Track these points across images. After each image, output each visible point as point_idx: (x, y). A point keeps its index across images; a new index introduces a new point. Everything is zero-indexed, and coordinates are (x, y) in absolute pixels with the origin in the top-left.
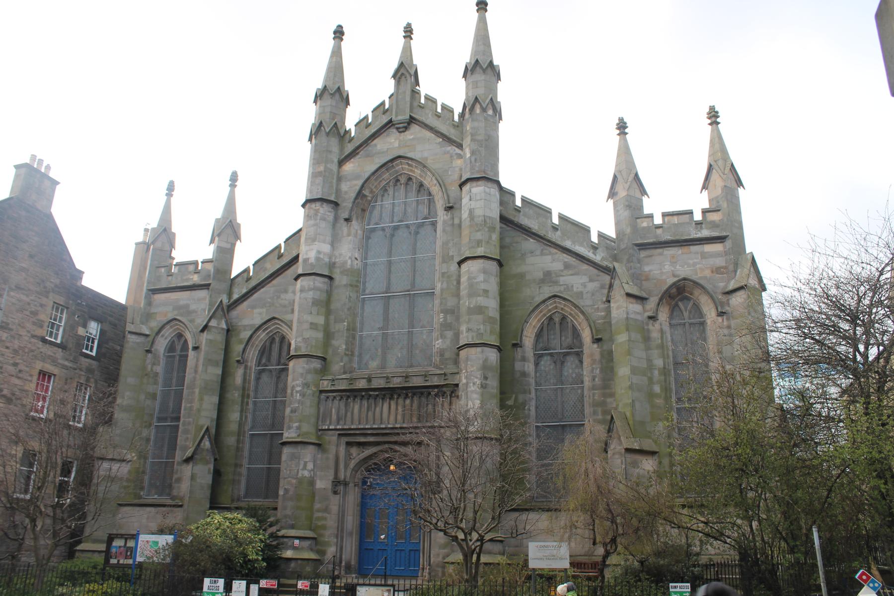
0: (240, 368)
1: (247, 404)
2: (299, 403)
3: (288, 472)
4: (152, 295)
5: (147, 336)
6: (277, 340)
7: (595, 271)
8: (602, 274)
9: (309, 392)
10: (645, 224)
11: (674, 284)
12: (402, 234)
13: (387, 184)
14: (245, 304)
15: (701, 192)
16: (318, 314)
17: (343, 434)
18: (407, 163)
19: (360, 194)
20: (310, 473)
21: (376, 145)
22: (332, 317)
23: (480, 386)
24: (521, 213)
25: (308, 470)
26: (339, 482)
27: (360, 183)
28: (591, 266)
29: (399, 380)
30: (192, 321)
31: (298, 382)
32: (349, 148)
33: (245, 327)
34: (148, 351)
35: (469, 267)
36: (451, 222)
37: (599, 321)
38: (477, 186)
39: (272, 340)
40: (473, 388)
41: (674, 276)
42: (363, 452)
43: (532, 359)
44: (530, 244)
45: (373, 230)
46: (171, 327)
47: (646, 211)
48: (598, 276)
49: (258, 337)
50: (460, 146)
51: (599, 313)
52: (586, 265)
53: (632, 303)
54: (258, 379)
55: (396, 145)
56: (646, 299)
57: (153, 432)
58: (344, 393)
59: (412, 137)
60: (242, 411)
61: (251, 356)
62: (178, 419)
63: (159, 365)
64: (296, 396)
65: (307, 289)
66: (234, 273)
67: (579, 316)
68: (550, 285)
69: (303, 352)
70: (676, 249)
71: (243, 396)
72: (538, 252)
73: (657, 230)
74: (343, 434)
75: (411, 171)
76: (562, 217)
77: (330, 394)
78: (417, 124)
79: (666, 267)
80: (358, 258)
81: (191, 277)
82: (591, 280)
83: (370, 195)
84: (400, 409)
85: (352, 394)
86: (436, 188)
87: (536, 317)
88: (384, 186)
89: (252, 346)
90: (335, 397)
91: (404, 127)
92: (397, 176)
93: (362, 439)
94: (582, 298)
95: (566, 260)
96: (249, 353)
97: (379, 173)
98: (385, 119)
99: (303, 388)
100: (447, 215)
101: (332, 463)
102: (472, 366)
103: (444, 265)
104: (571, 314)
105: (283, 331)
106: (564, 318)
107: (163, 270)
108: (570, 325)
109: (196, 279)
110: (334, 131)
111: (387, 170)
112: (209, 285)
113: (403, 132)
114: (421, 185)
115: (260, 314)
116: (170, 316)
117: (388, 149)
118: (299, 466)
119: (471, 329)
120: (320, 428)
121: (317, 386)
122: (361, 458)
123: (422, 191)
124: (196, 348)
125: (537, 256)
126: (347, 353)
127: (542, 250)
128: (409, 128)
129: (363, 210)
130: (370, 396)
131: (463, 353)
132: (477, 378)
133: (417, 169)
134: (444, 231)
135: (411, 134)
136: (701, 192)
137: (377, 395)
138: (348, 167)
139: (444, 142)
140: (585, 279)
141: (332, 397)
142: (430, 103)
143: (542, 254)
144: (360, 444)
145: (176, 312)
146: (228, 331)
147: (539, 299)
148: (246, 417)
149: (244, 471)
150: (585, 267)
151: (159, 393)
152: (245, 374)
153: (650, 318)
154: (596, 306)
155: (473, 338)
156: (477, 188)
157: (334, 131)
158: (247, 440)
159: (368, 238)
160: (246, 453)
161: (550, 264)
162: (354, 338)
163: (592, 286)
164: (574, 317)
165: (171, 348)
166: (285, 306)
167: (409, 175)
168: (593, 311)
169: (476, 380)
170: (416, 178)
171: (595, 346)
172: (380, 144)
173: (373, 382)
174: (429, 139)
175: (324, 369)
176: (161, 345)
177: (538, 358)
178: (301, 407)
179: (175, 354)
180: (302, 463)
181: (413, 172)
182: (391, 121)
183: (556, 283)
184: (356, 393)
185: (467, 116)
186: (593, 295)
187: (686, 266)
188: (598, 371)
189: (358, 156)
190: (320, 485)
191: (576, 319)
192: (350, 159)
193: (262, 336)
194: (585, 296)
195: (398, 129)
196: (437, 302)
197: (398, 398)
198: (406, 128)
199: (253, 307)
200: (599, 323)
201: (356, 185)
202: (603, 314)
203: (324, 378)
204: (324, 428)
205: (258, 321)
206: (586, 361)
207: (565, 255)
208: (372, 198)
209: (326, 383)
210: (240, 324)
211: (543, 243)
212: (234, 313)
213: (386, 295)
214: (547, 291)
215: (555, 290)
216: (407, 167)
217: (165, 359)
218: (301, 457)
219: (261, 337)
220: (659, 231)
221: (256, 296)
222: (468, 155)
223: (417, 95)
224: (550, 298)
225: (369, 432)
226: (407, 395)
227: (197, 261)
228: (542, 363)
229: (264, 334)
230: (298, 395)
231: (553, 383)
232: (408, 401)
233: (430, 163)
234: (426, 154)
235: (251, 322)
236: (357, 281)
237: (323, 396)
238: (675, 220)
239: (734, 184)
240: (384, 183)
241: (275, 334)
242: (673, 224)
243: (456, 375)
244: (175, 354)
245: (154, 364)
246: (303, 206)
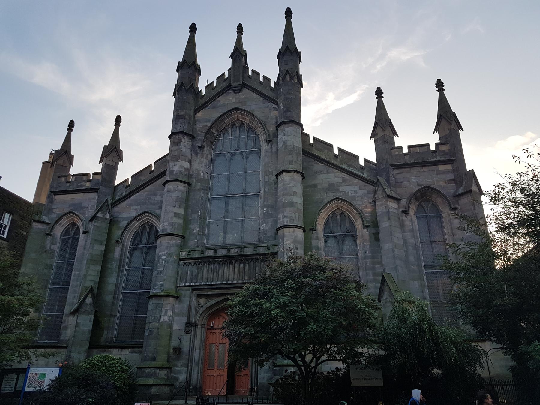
0: (118, 247)
1: (123, 271)
2: (164, 268)
3: (153, 318)
4: (54, 196)
5: (48, 224)
6: (147, 227)
7: (364, 183)
8: (367, 185)
9: (172, 259)
10: (397, 153)
11: (419, 190)
12: (238, 158)
13: (227, 126)
17: (195, 288)
19: (209, 131)
20: (170, 318)
21: (219, 101)
22: (190, 210)
24: (314, 148)
25: (168, 316)
26: (191, 324)
27: (209, 124)
28: (360, 180)
29: (236, 250)
30: (84, 214)
31: (163, 253)
32: (201, 102)
33: (124, 219)
34: (48, 235)
35: (286, 177)
36: (270, 151)
37: (367, 215)
39: (143, 227)
41: (418, 185)
42: (209, 301)
43: (323, 239)
44: (320, 166)
45: (218, 155)
46: (67, 218)
47: (397, 145)
48: (365, 186)
49: (134, 225)
50: (276, 103)
51: (367, 210)
53: (391, 202)
54: (132, 254)
56: (401, 200)
57: (48, 292)
58: (197, 261)
59: (244, 96)
60: (118, 276)
61: (127, 238)
62: (69, 283)
63: (56, 245)
64: (162, 262)
65: (172, 190)
66: (117, 183)
67: (353, 212)
69: (169, 231)
70: (419, 168)
71: (120, 266)
72: (325, 172)
73: (405, 156)
74: (195, 288)
75: (243, 118)
77: (187, 261)
79: (413, 180)
80: (208, 172)
81: (85, 184)
83: (216, 133)
84: (236, 270)
85: (204, 260)
86: (260, 129)
87: (325, 212)
88: (225, 128)
89: (129, 231)
90: (190, 263)
91: (238, 90)
93: (209, 292)
94: (355, 200)
95: (344, 176)
96: (126, 236)
98: (225, 85)
99: (168, 257)
100: (268, 146)
101: (185, 310)
102: (287, 240)
103: (267, 177)
104: (347, 210)
105: (153, 221)
106: (343, 213)
107: (63, 179)
108: (347, 217)
109: (88, 185)
112: (99, 189)
113: (238, 93)
114: (250, 128)
115: (136, 209)
116: (67, 210)
117: (228, 103)
118: (162, 314)
119: (286, 217)
120: (179, 285)
123: (250, 132)
124: (85, 232)
126: (200, 233)
127: (328, 170)
128: (242, 91)
129: (212, 143)
130: (216, 261)
131: (280, 232)
133: (248, 117)
134: (266, 156)
137: (221, 261)
138: (199, 114)
139: (265, 100)
140: (356, 188)
141: (188, 263)
142: (255, 75)
143: (328, 173)
144: (207, 296)
145: (71, 208)
146: (111, 220)
147: (326, 201)
148: (121, 281)
149: (117, 320)
150: (357, 180)
153: (403, 212)
154: (365, 205)
155: (287, 222)
156: (288, 128)
158: (121, 297)
159: (215, 160)
160: (119, 306)
161: (333, 179)
162: (205, 223)
163: (361, 192)
164: (350, 212)
165: (66, 233)
166: (154, 204)
168: (363, 208)
170: (247, 123)
171: (366, 230)
172: (222, 100)
173: (218, 252)
174: (255, 98)
176: (59, 231)
177: (327, 238)
178: (165, 270)
179: (69, 237)
180: (164, 311)
181: (245, 119)
182: (230, 85)
183: (338, 191)
185: (281, 83)
186: (362, 198)
188: (368, 247)
189: (208, 107)
190: (175, 327)
194: (357, 199)
195: (234, 91)
196: (262, 200)
197: (235, 263)
198: (240, 91)
199: (131, 205)
200: (367, 216)
201: (206, 126)
202: (369, 210)
203: (182, 250)
204: (181, 285)
205: (134, 214)
207: (343, 173)
208: (217, 135)
209: (184, 253)
210: (120, 216)
211: (329, 166)
212: (116, 209)
213: (227, 196)
214: (331, 196)
215: (338, 195)
216: (241, 116)
217: (61, 240)
218: (164, 307)
220: (407, 158)
222: (282, 107)
223: (247, 70)
227: (90, 173)
230: (164, 262)
231: (337, 255)
232: (242, 265)
233: (256, 113)
234: (253, 107)
235: (129, 215)
236: (207, 187)
237: (182, 262)
238: (418, 150)
240: (225, 125)
242: (417, 153)
243: (276, 246)
244: (69, 237)
245: (52, 244)
246: (170, 137)
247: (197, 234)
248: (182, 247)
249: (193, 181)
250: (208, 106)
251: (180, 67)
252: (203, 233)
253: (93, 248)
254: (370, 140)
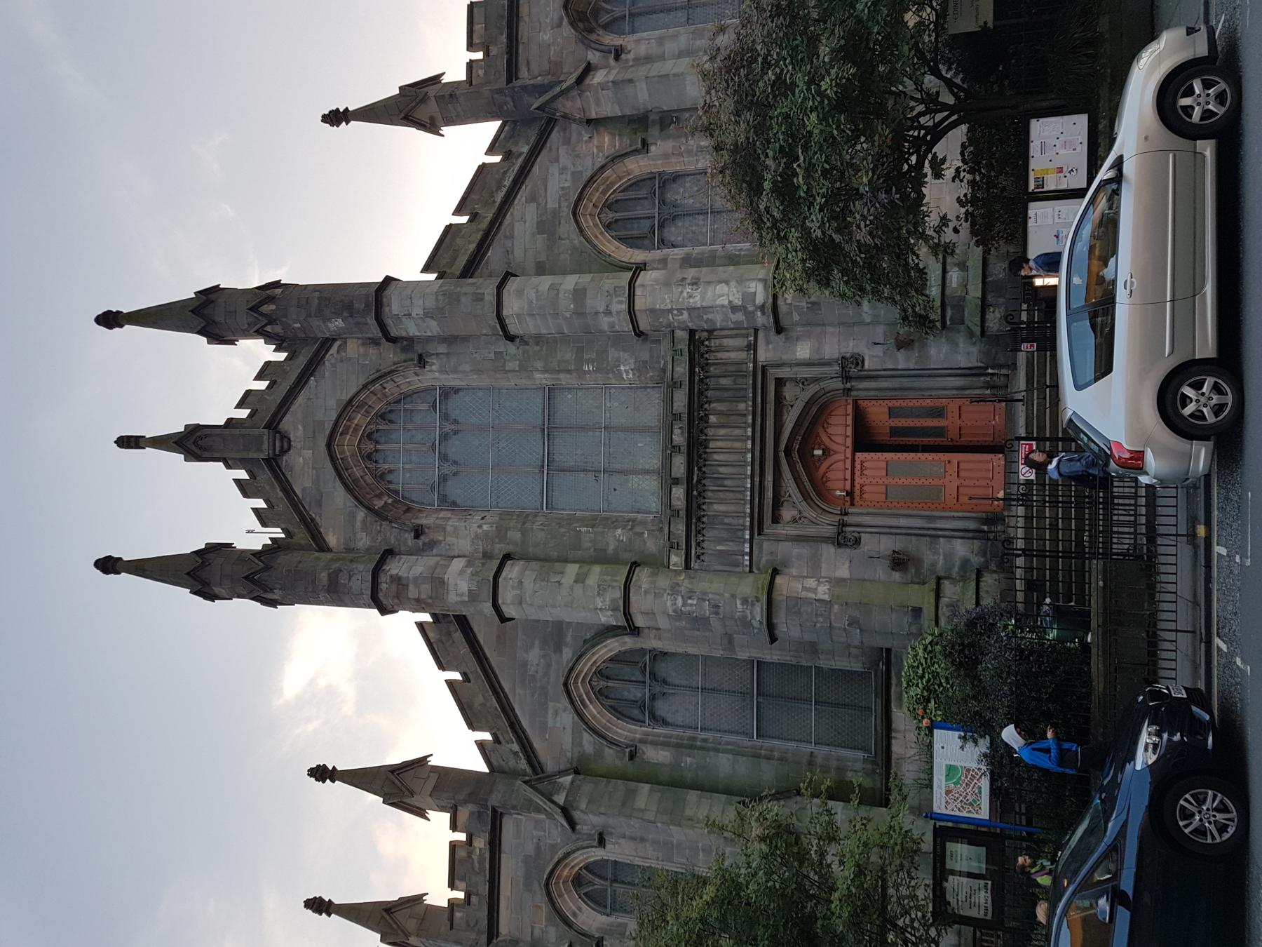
0: (644, 753)
1: (705, 741)
2: (704, 600)
3: (821, 619)
6: (602, 684)
7: (544, 153)
8: (548, 145)
9: (686, 583)
10: (481, 72)
11: (572, 24)
12: (455, 447)
13: (372, 474)
14: (537, 744)
16: (562, 573)
17: (758, 527)
18: (341, 434)
20: (822, 583)
21: (304, 490)
23: (695, 287)
25: (818, 586)
26: (839, 534)
27: (361, 514)
28: (535, 160)
29: (677, 431)
30: (554, 848)
31: (669, 604)
32: (301, 536)
33: (577, 742)
35: (512, 306)
36: (444, 358)
37: (617, 144)
38: (389, 305)
39: (601, 695)
40: (698, 298)
41: (560, 25)
42: (790, 496)
43: (666, 251)
45: (443, 499)
47: (461, 75)
48: (550, 149)
49: (594, 717)
50: (327, 343)
51: (606, 145)
52: (534, 168)
53: (593, 78)
54: (665, 723)
55: (308, 453)
56: (589, 63)
58: (693, 527)
59: (300, 428)
60: (717, 750)
61: (625, 733)
63: (627, 924)
64: (691, 605)
67: (608, 178)
68: (557, 223)
69: (618, 594)
70: (521, 24)
71: (692, 747)
72: (508, 243)
73: (491, 54)
74: (758, 527)
75: (356, 430)
76: (458, 211)
77: (693, 552)
78: (281, 419)
79: (546, 38)
82: (557, 160)
84: (722, 432)
85: (694, 511)
86: (389, 386)
87: (603, 244)
88: (375, 477)
89: (608, 729)
90: (698, 544)
92: (362, 457)
93: (769, 494)
94: (581, 172)
95: (524, 198)
96: (620, 736)
97: (349, 481)
98: (265, 475)
99: (678, 593)
100: (433, 364)
101: (804, 550)
102: (663, 300)
103: (509, 366)
104: (604, 193)
105: (589, 670)
106: (610, 206)
108: (619, 196)
109: (480, 843)
110: (266, 558)
111: (347, 469)
112: (494, 810)
114: (382, 416)
115: (556, 713)
116: (541, 898)
117: (313, 468)
118: (810, 598)
119: (607, 306)
120: (748, 569)
121: (677, 573)
122: (801, 498)
123: (392, 417)
124: (602, 842)
125: (513, 244)
127: (506, 237)
128: (286, 432)
129: (408, 509)
130: (699, 481)
131: (644, 324)
132: (682, 292)
133: (354, 419)
134: (455, 371)
135: (296, 429)
137: (700, 469)
138: (332, 540)
139: (316, 373)
140: (554, 170)
141: (698, 548)
142: (249, 399)
143: (512, 237)
144: (777, 504)
145: (536, 884)
146: (577, 772)
147: (577, 240)
148: (728, 743)
149: (821, 751)
150: (536, 169)
152: (653, 743)
153: (617, 58)
154: (595, 150)
155: (621, 302)
156: (393, 306)
157: (266, 558)
158: (768, 743)
159: (454, 504)
160: (791, 745)
161: (527, 224)
162: (607, 519)
163: (565, 160)
164: (609, 187)
165: (597, 901)
166: (549, 665)
167: (362, 436)
168: (601, 154)
169: (685, 294)
170: (369, 424)
171: (653, 148)
172: (302, 483)
173: (678, 475)
174: (309, 399)
177: (663, 243)
178: (710, 596)
180: (804, 594)
183: (556, 213)
184: (694, 506)
185: (278, 329)
186: (578, 156)
187: (548, 9)
188: (691, 142)
189: (318, 519)
190: (843, 572)
191: (613, 184)
192: (320, 533)
193: (593, 710)
194: (580, 169)
195: (284, 452)
196: (564, 379)
197: (706, 435)
198: (285, 437)
199: (544, 727)
200: (620, 145)
201: (364, 522)
202: (606, 139)
203: (666, 564)
204: (748, 563)
205: (567, 718)
206: (676, 166)
207: (516, 202)
208: (390, 496)
209: (674, 559)
210: (569, 755)
211: (495, 235)
212: (550, 765)
213: (546, 468)
214: (567, 228)
215: (566, 212)
216: (348, 437)
217: (617, 914)
218: (795, 595)
219: (596, 713)
220: (494, 51)
221: (525, 723)
222: (339, 323)
223: (234, 422)
224: (577, 222)
225: (757, 479)
226: (701, 419)
228: (672, 239)
229: (591, 707)
230: (690, 601)
231: (703, 220)
232: (712, 419)
233: (345, 397)
234: (332, 403)
235: (569, 731)
238: (479, 27)
240: (369, 479)
241: (592, 688)
242: (486, 30)
243: (675, 335)
247: (631, 533)
248: (658, 564)
249: (500, 549)
250: (313, 520)
252: (628, 521)
253: (643, 811)
254: (443, 136)
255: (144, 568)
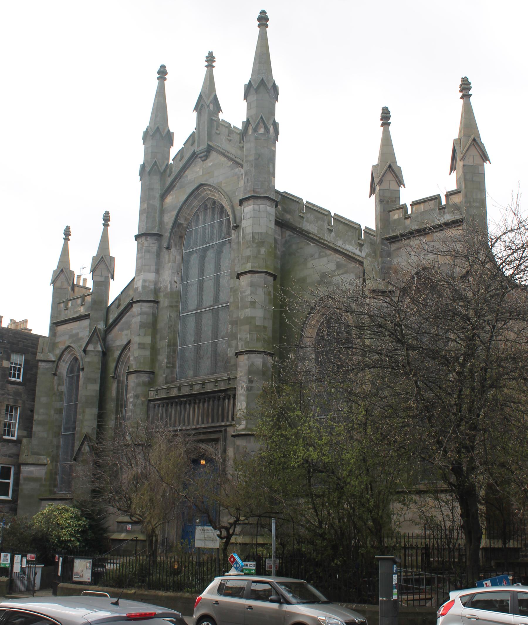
4: (56, 327)
5: (53, 362)
9: (139, 402)
13: (198, 210)
14: (117, 327)
15: (450, 174)
19: (176, 224)
21: (187, 176)
22: (158, 336)
23: (246, 389)
24: (305, 220)
27: (175, 213)
34: (55, 374)
36: (236, 241)
40: (241, 392)
44: (311, 248)
46: (69, 353)
55: (201, 173)
57: (62, 439)
62: (74, 429)
63: (63, 385)
65: (136, 314)
66: (110, 303)
72: (317, 256)
73: (406, 220)
75: (214, 196)
77: (156, 402)
80: (178, 282)
81: (79, 309)
83: (186, 223)
89: (123, 363)
91: (204, 156)
92: (204, 202)
95: (338, 260)
96: (121, 370)
97: (189, 201)
99: (134, 399)
102: (241, 372)
107: (62, 305)
111: (195, 198)
112: (89, 315)
113: (206, 160)
116: (67, 344)
117: (195, 178)
125: (316, 259)
126: (169, 366)
127: (320, 253)
129: (181, 237)
130: (181, 402)
132: (244, 382)
136: (450, 174)
137: (186, 401)
138: (169, 200)
143: (320, 257)
151: (64, 408)
152: (118, 387)
162: (175, 352)
165: (71, 370)
169: (243, 384)
173: (182, 390)
175: (151, 383)
176: (64, 368)
178: (133, 415)
179: (73, 375)
181: (214, 196)
182: (194, 153)
189: (176, 188)
195: (201, 158)
198: (207, 157)
199: (122, 330)
207: (337, 255)
213: (197, 311)
221: (124, 320)
230: (131, 405)
236: (177, 302)
237: (152, 404)
238: (422, 207)
239: (479, 160)
240: (195, 209)
244: (73, 375)
245: (59, 384)
247: (165, 367)
250: (175, 186)
251: (147, 136)
252: (172, 364)
253: (86, 388)
255: (161, 94)
